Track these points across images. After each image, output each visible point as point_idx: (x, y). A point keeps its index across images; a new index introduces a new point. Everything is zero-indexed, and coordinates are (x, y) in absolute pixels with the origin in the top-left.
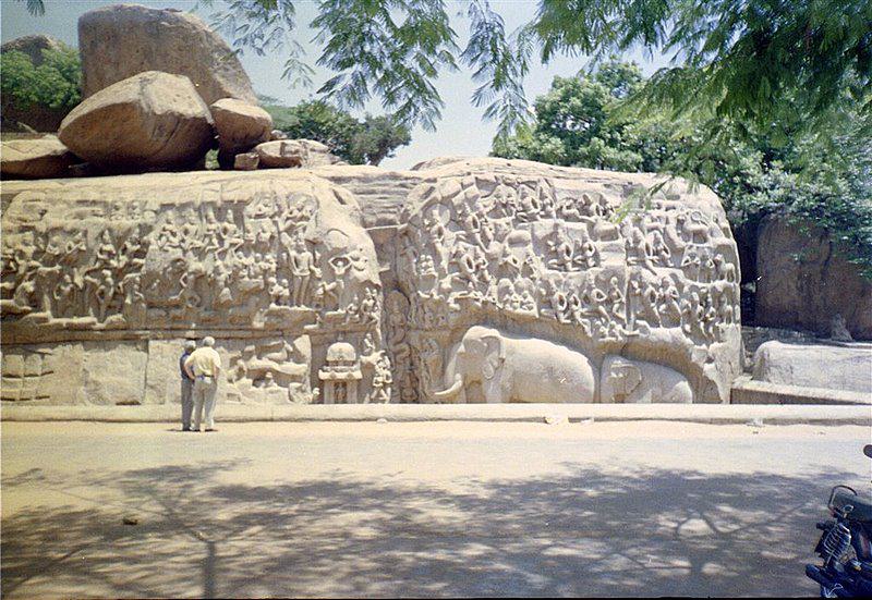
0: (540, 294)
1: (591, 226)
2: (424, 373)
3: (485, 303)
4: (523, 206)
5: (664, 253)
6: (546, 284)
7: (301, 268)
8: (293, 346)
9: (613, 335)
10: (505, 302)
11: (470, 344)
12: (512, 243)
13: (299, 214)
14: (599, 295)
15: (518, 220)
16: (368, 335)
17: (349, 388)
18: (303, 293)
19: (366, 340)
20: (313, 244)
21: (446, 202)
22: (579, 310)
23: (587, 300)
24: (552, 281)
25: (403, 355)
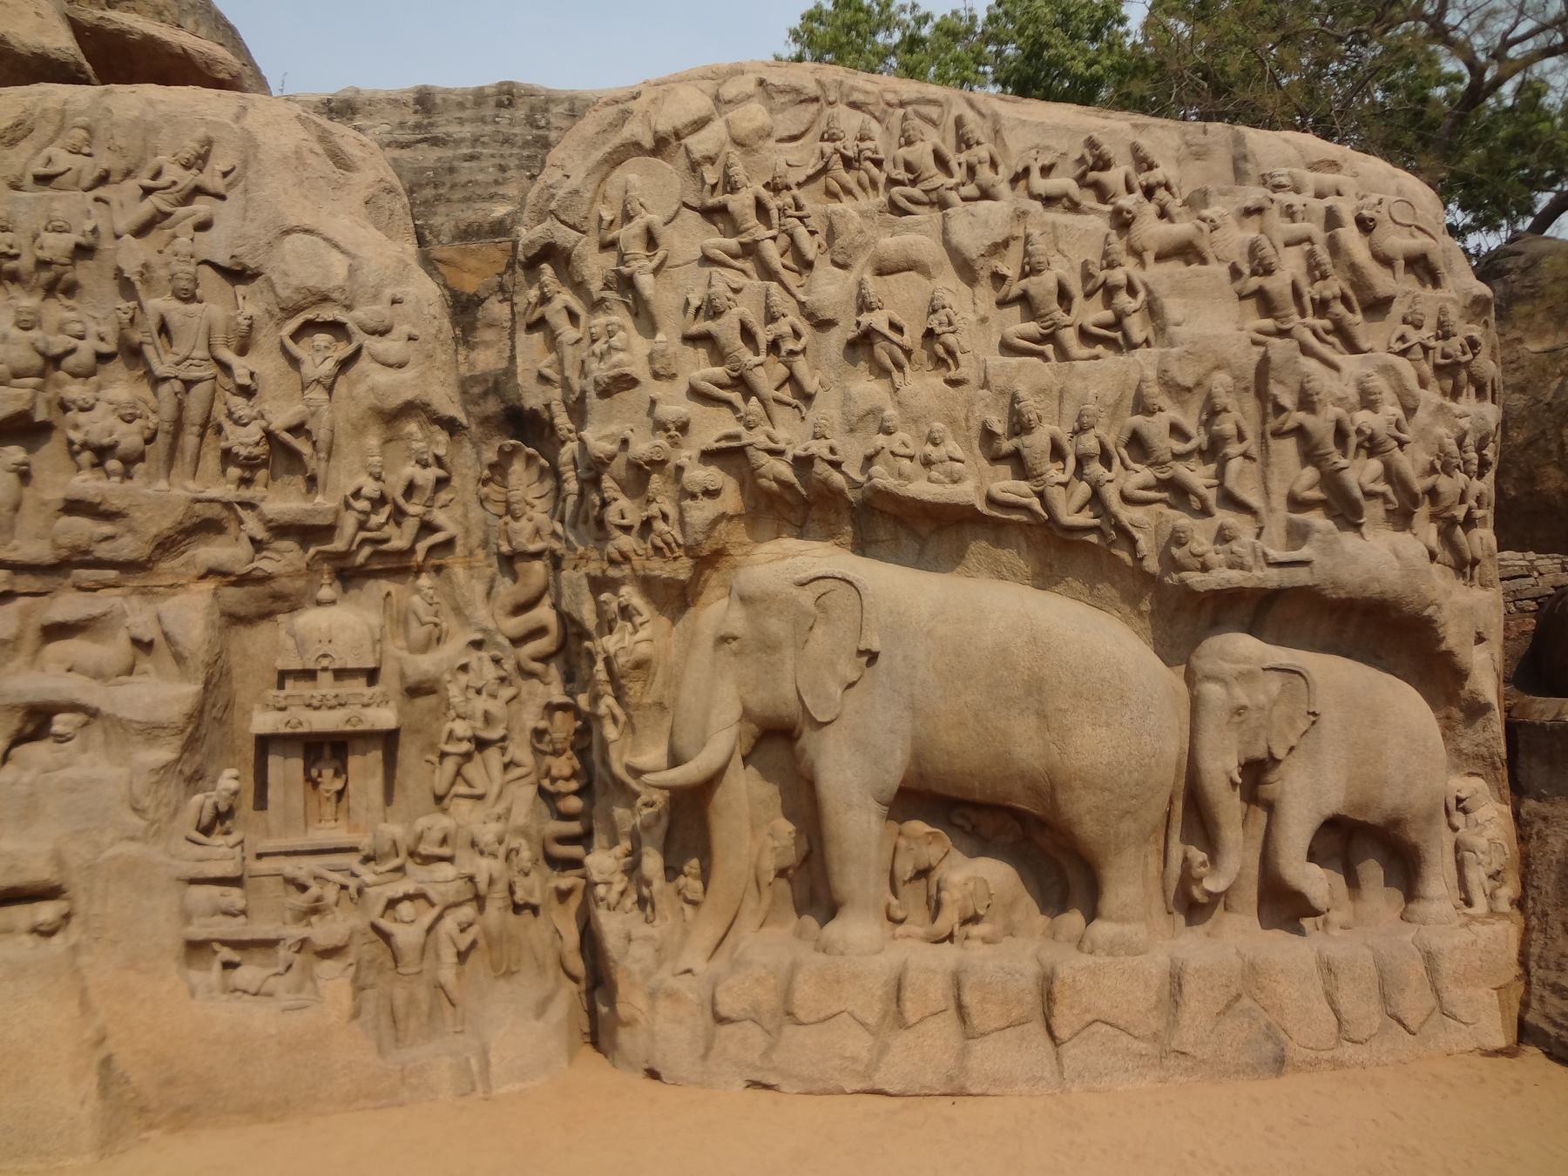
0: (988, 435)
1: (1122, 221)
2: (608, 701)
3: (803, 464)
4: (909, 167)
5: (1338, 308)
7: (182, 349)
8: (159, 619)
10: (869, 460)
13: (188, 179)
14: (1176, 431)
16: (425, 581)
18: (190, 440)
20: (237, 275)
23: (1137, 444)
24: (1022, 390)
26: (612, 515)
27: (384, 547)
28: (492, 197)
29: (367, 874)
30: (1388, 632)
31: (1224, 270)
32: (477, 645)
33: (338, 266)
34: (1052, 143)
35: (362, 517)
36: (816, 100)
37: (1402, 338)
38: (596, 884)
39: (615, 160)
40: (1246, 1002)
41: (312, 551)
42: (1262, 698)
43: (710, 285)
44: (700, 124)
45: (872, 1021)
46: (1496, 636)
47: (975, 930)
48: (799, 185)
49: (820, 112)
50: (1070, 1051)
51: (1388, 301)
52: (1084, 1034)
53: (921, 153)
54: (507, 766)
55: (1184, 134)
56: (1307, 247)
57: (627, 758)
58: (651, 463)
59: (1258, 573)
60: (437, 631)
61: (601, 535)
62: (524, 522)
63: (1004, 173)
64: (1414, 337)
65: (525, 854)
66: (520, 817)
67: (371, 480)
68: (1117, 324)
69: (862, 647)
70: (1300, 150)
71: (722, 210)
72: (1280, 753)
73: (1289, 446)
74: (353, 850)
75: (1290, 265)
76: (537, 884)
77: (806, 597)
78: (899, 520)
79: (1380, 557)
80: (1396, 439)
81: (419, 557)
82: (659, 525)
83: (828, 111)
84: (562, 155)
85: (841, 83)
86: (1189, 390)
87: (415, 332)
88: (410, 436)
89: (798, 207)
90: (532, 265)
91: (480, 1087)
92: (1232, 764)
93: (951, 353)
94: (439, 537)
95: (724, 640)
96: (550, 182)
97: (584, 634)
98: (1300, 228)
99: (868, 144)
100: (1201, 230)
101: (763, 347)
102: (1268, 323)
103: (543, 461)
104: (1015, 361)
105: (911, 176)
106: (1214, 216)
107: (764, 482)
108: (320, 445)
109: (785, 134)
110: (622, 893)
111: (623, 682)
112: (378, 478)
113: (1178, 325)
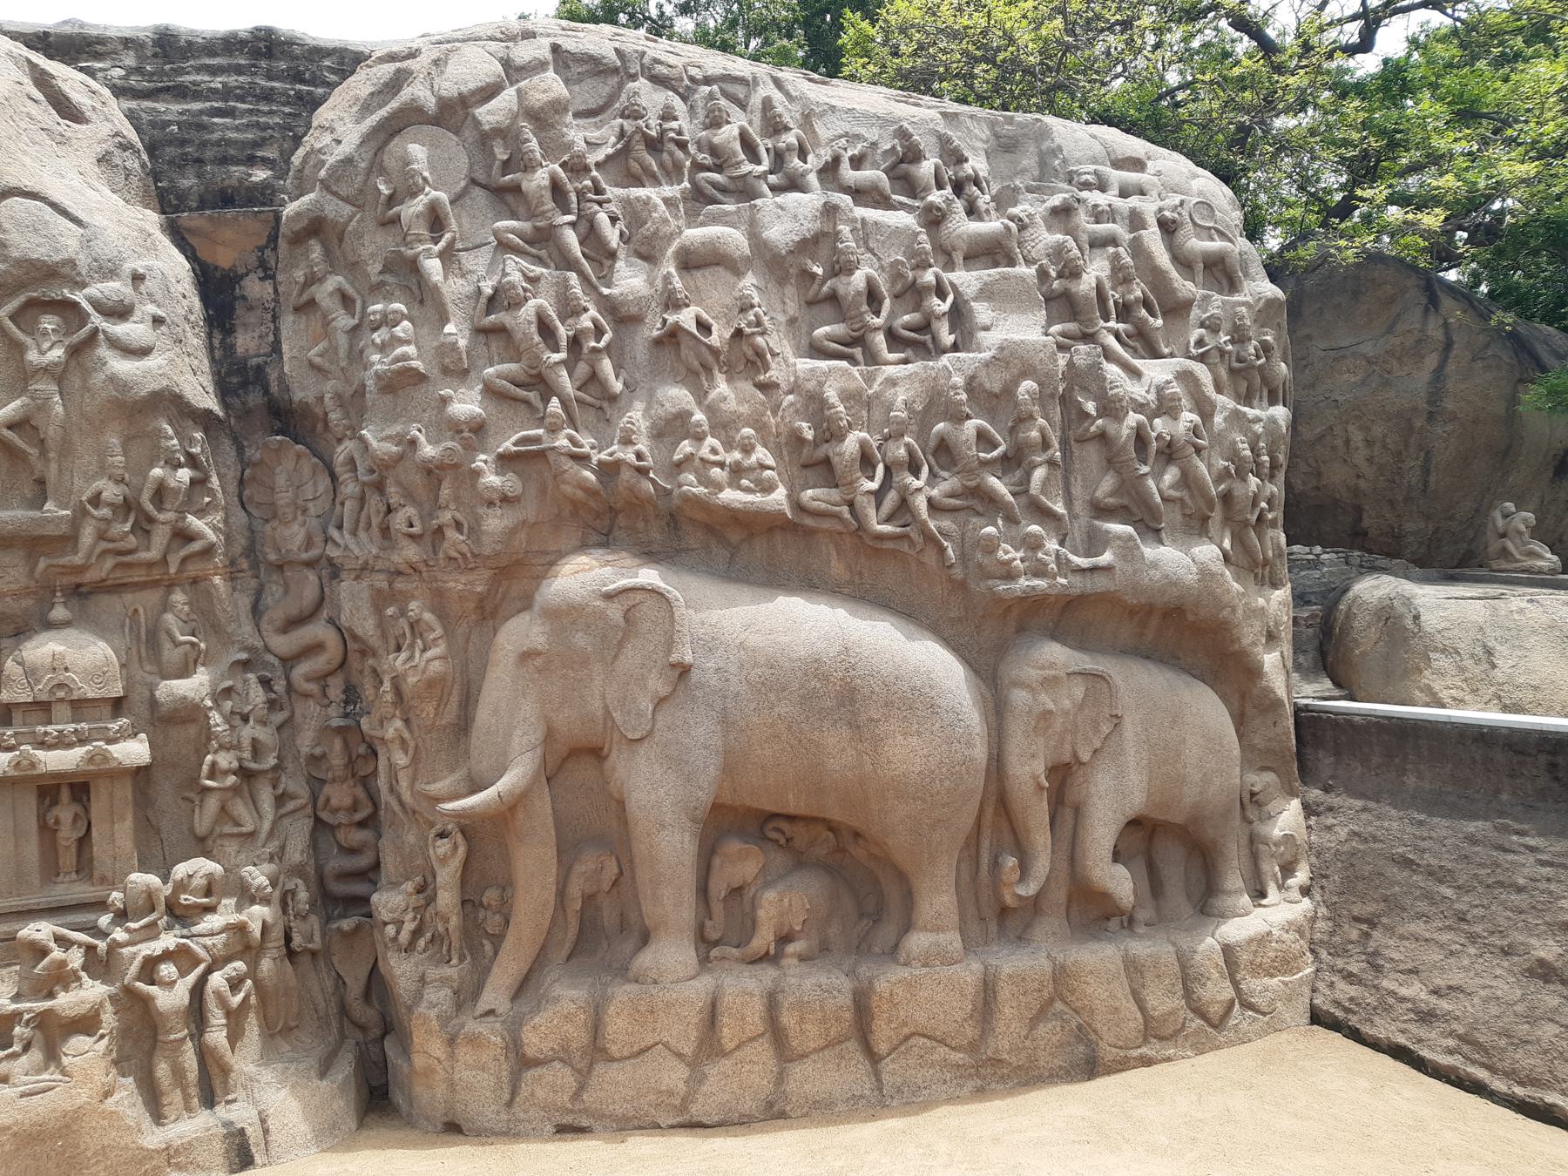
0: (797, 439)
1: (934, 219)
2: (394, 727)
3: (609, 470)
4: (714, 150)
6: (815, 405)
9: (1039, 571)
10: (679, 466)
11: (565, 616)
12: (690, 262)
15: (699, 197)
16: (178, 597)
17: (98, 807)
19: (169, 617)
21: (453, 113)
22: (922, 489)
23: (944, 452)
24: (831, 394)
25: (318, 663)
26: (398, 521)
27: (128, 559)
28: (251, 161)
29: (119, 935)
30: (1188, 636)
31: (1032, 270)
32: (245, 665)
33: (67, 242)
34: (862, 131)
35: (103, 526)
36: (616, 71)
37: (1200, 343)
38: (386, 924)
39: (391, 129)
40: (1059, 1006)
41: (42, 564)
42: (1067, 703)
43: (505, 274)
44: (489, 92)
45: (688, 1050)
46: (1286, 633)
47: (791, 948)
48: (598, 165)
49: (621, 86)
50: (889, 1067)
51: (1187, 305)
52: (903, 1048)
53: (727, 134)
54: (280, 800)
55: (992, 124)
56: (1111, 250)
57: (419, 786)
58: (441, 467)
59: (1063, 581)
60: (193, 656)
61: (386, 544)
62: (296, 527)
63: (813, 162)
64: (1211, 343)
65: (303, 895)
66: (297, 851)
67: (111, 484)
68: (925, 327)
69: (674, 658)
70: (1104, 144)
71: (516, 189)
72: (1085, 756)
73: (1091, 455)
74: (101, 905)
75: (1096, 270)
76: (317, 927)
77: (615, 612)
78: (709, 529)
79: (1183, 560)
80: (1195, 446)
81: (172, 570)
82: (451, 534)
83: (631, 85)
84: (331, 115)
85: (643, 54)
86: (996, 396)
87: (160, 313)
88: (159, 433)
89: (598, 190)
90: (299, 239)
91: (258, 1159)
92: (1039, 767)
93: (759, 354)
94: (196, 546)
95: (526, 656)
96: (318, 146)
97: (366, 652)
98: (1104, 228)
99: (674, 125)
100: (1007, 228)
101: (564, 343)
102: (1071, 327)
103: (315, 460)
104: (824, 364)
105: (718, 162)
106: (1022, 215)
107: (568, 489)
108: (50, 443)
109: (582, 107)
110: (417, 933)
111: (415, 703)
112: (120, 481)
113: (986, 329)
